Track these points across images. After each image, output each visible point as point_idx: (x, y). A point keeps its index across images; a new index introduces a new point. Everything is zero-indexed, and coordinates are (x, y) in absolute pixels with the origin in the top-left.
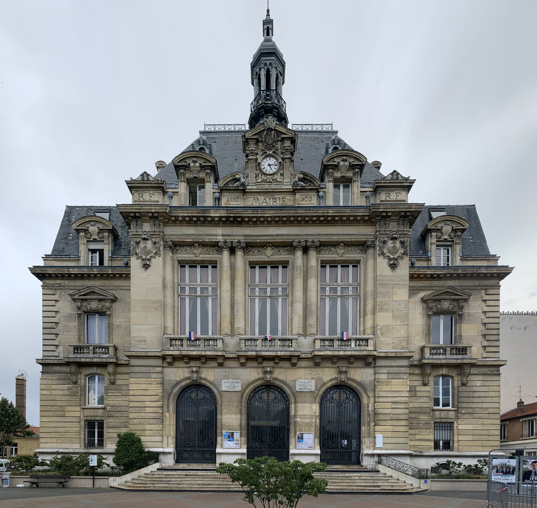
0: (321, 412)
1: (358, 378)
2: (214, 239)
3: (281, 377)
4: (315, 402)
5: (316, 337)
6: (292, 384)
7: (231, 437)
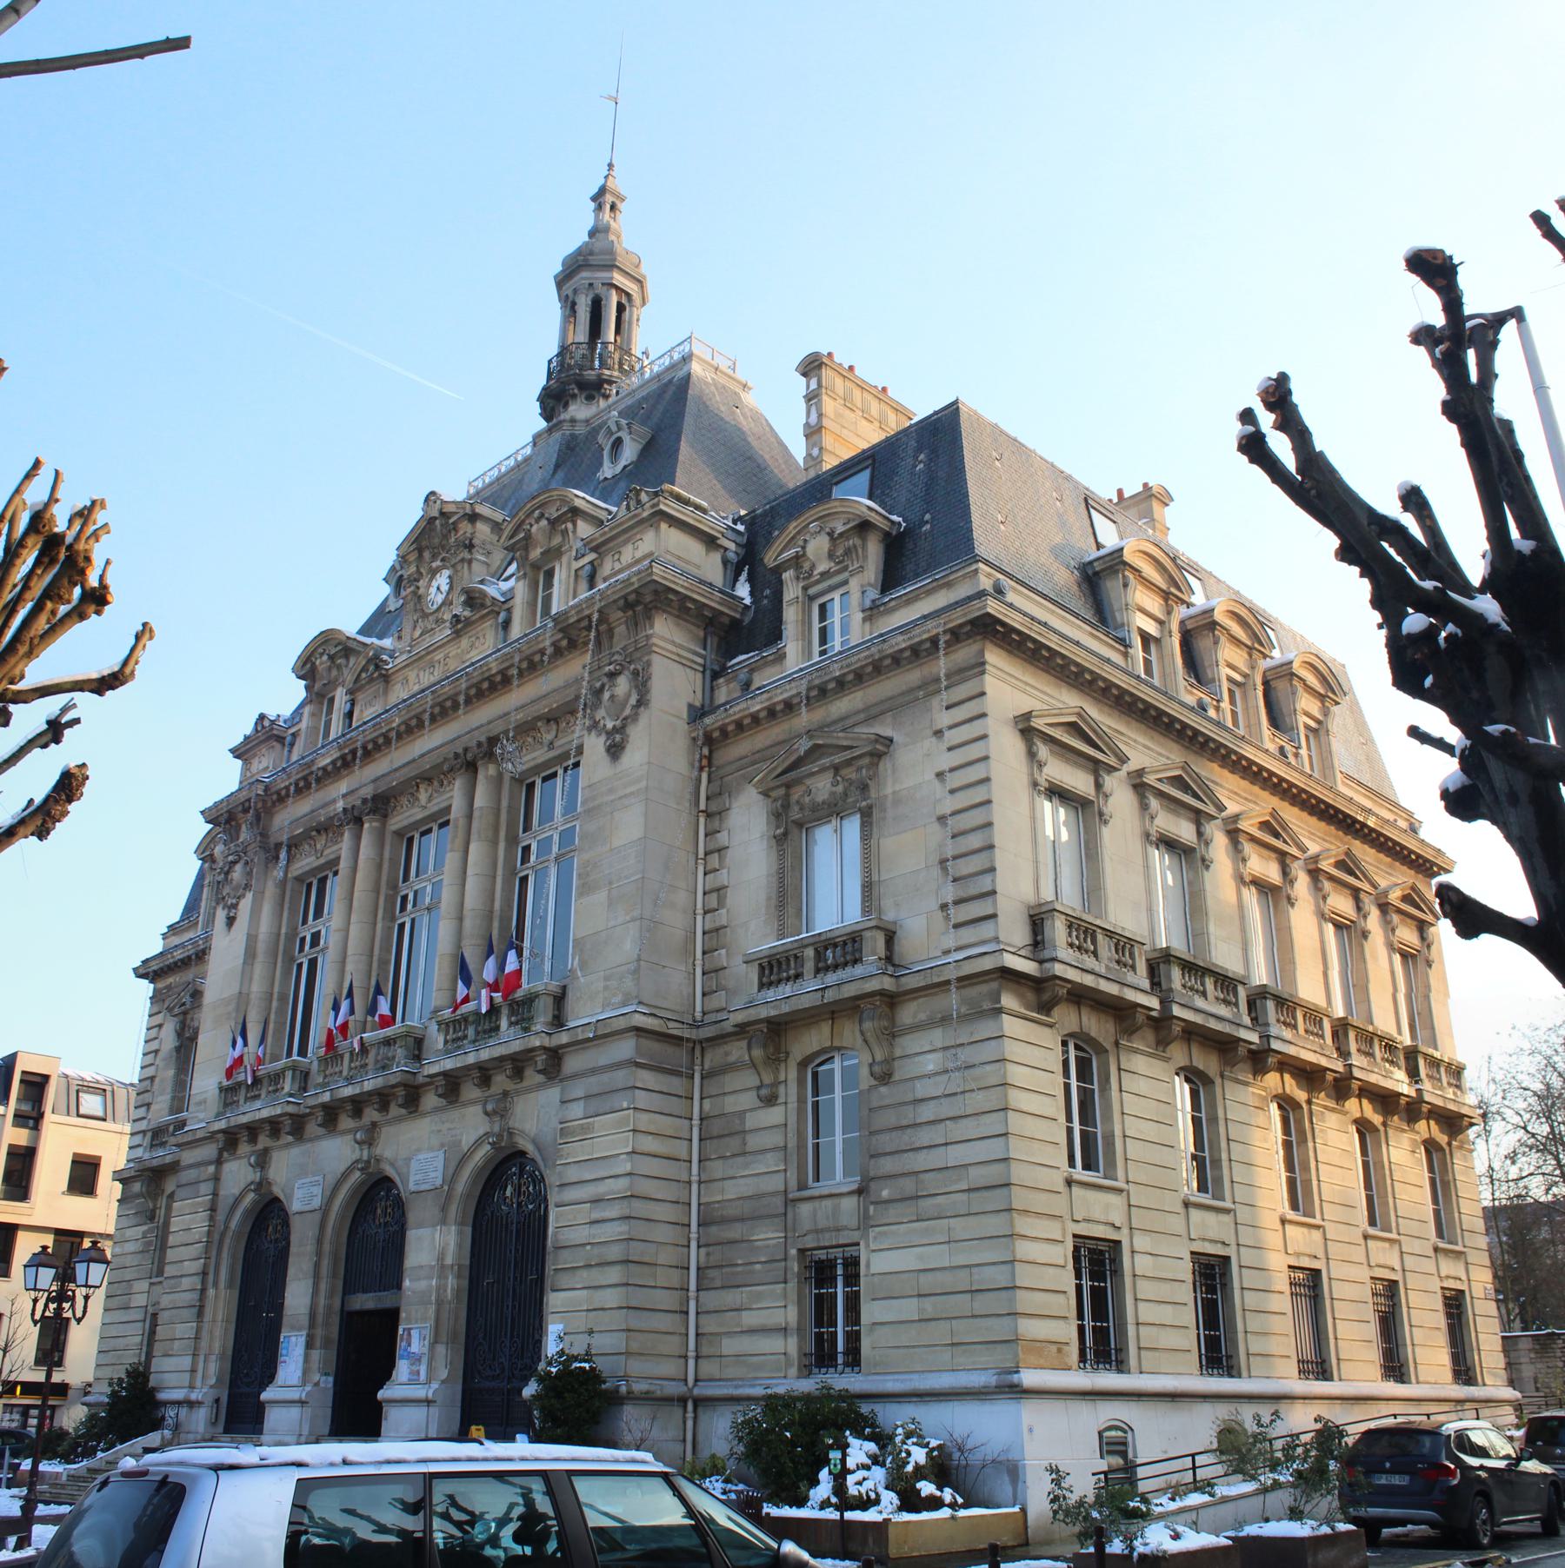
4: (444, 1222)
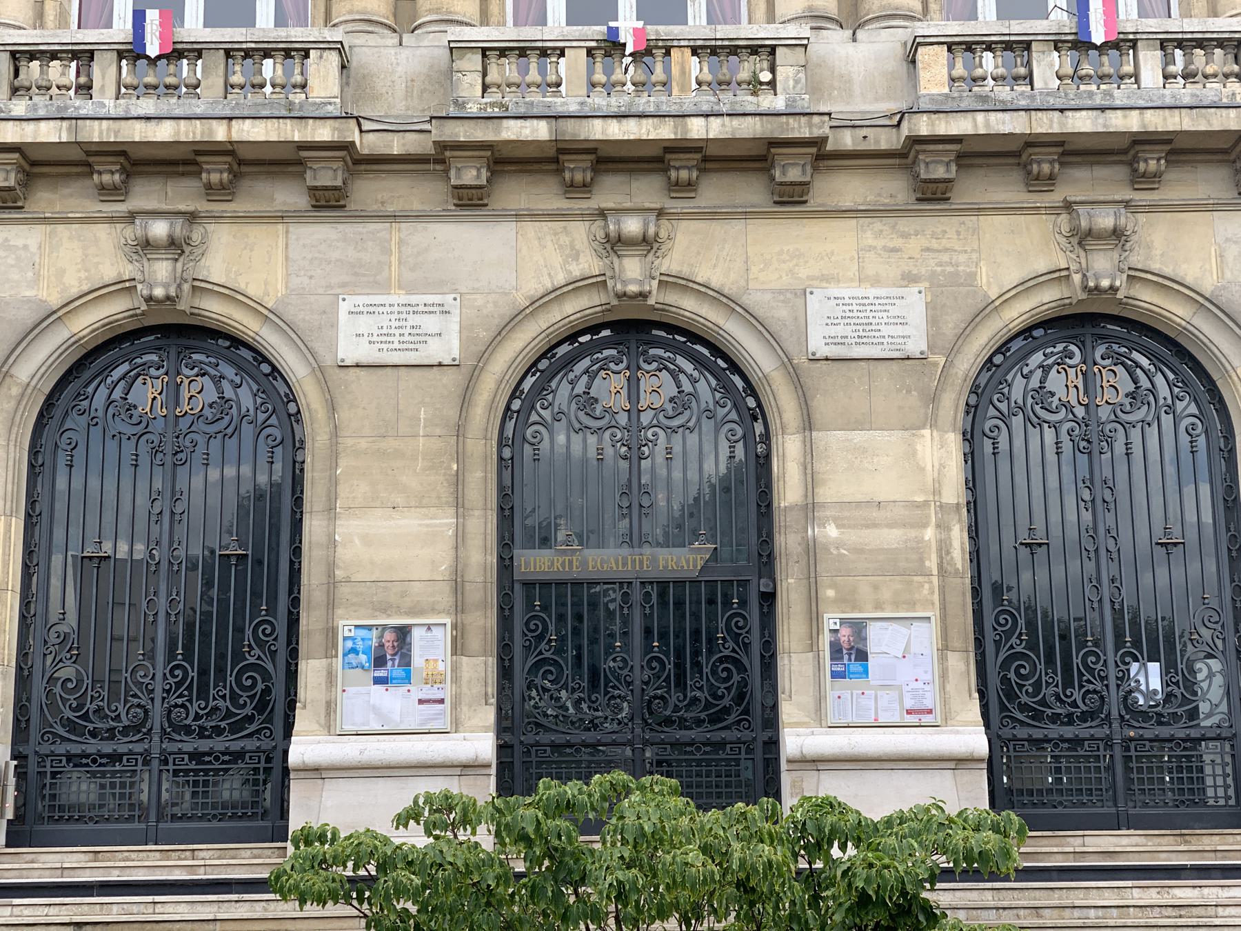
0: (972, 484)
3: (705, 273)
4: (934, 425)
5: (922, 29)
6: (783, 313)
7: (391, 655)
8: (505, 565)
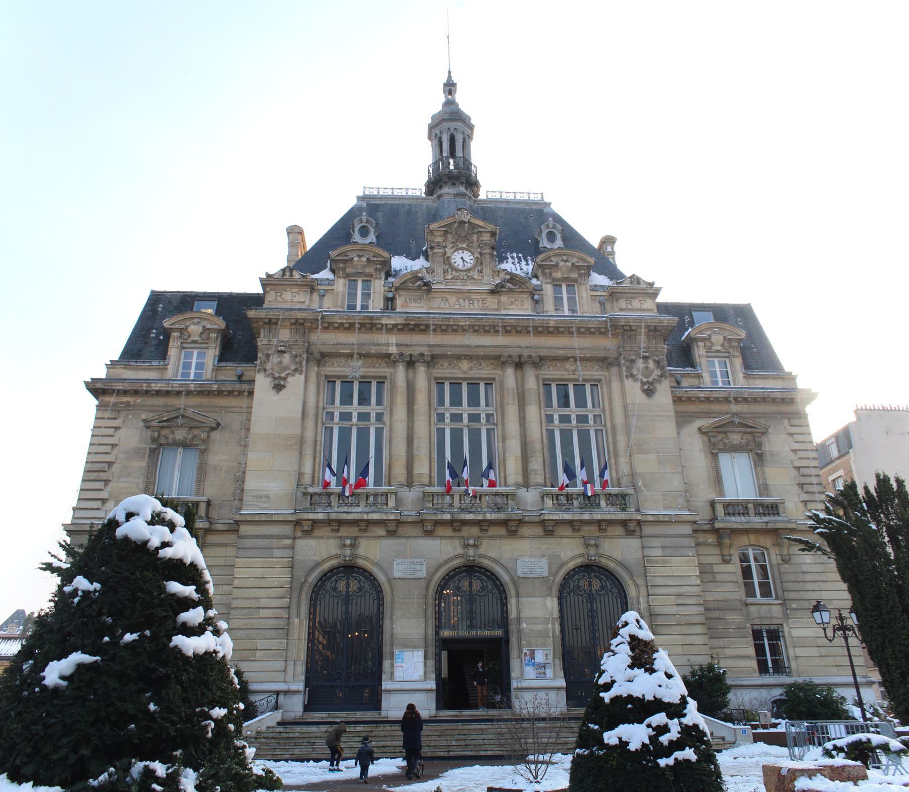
0: (561, 611)
1: (617, 555)
2: (384, 350)
3: (491, 554)
4: (550, 595)
8: (437, 633)
